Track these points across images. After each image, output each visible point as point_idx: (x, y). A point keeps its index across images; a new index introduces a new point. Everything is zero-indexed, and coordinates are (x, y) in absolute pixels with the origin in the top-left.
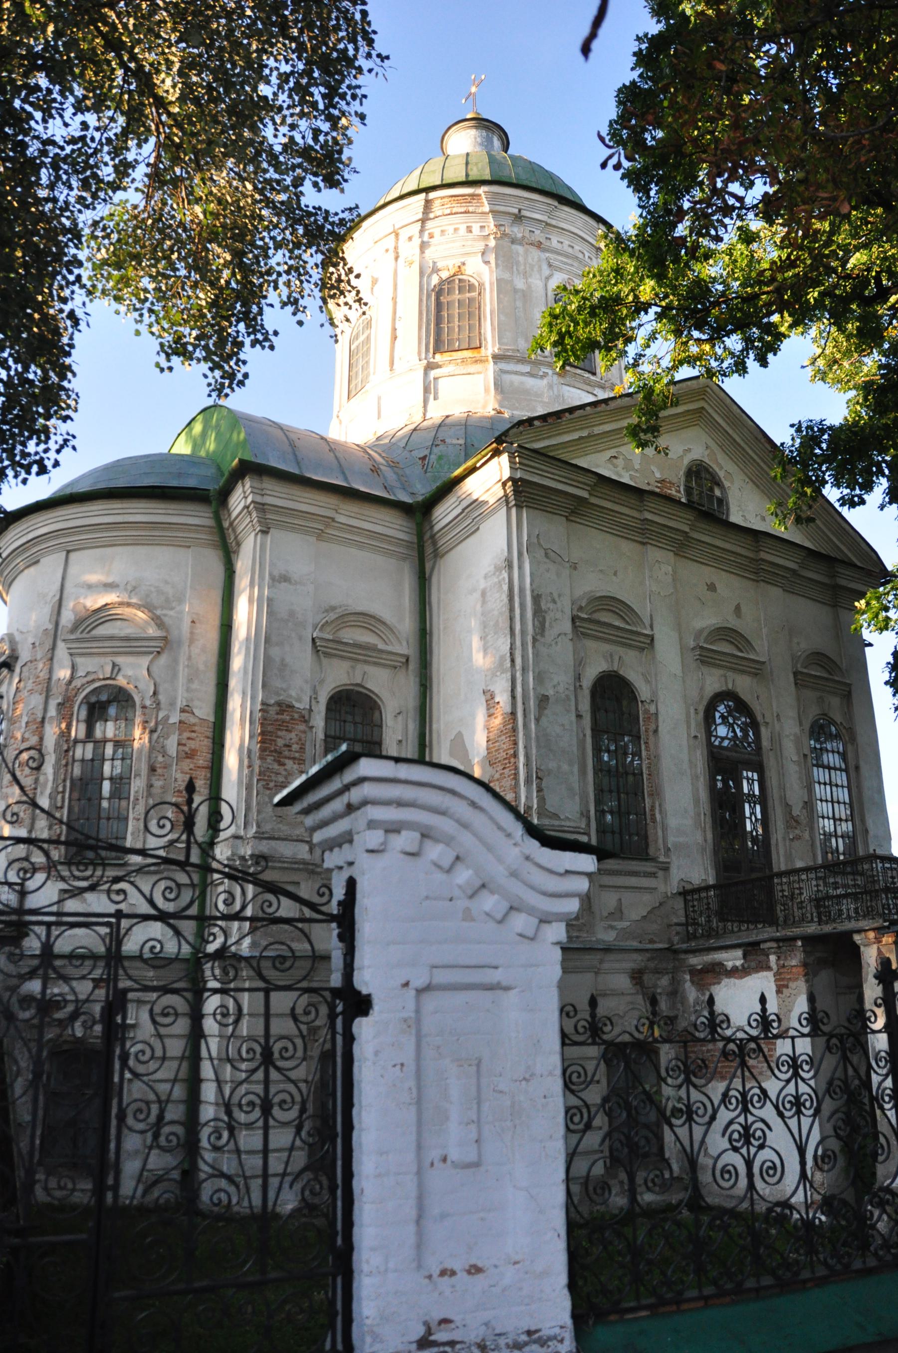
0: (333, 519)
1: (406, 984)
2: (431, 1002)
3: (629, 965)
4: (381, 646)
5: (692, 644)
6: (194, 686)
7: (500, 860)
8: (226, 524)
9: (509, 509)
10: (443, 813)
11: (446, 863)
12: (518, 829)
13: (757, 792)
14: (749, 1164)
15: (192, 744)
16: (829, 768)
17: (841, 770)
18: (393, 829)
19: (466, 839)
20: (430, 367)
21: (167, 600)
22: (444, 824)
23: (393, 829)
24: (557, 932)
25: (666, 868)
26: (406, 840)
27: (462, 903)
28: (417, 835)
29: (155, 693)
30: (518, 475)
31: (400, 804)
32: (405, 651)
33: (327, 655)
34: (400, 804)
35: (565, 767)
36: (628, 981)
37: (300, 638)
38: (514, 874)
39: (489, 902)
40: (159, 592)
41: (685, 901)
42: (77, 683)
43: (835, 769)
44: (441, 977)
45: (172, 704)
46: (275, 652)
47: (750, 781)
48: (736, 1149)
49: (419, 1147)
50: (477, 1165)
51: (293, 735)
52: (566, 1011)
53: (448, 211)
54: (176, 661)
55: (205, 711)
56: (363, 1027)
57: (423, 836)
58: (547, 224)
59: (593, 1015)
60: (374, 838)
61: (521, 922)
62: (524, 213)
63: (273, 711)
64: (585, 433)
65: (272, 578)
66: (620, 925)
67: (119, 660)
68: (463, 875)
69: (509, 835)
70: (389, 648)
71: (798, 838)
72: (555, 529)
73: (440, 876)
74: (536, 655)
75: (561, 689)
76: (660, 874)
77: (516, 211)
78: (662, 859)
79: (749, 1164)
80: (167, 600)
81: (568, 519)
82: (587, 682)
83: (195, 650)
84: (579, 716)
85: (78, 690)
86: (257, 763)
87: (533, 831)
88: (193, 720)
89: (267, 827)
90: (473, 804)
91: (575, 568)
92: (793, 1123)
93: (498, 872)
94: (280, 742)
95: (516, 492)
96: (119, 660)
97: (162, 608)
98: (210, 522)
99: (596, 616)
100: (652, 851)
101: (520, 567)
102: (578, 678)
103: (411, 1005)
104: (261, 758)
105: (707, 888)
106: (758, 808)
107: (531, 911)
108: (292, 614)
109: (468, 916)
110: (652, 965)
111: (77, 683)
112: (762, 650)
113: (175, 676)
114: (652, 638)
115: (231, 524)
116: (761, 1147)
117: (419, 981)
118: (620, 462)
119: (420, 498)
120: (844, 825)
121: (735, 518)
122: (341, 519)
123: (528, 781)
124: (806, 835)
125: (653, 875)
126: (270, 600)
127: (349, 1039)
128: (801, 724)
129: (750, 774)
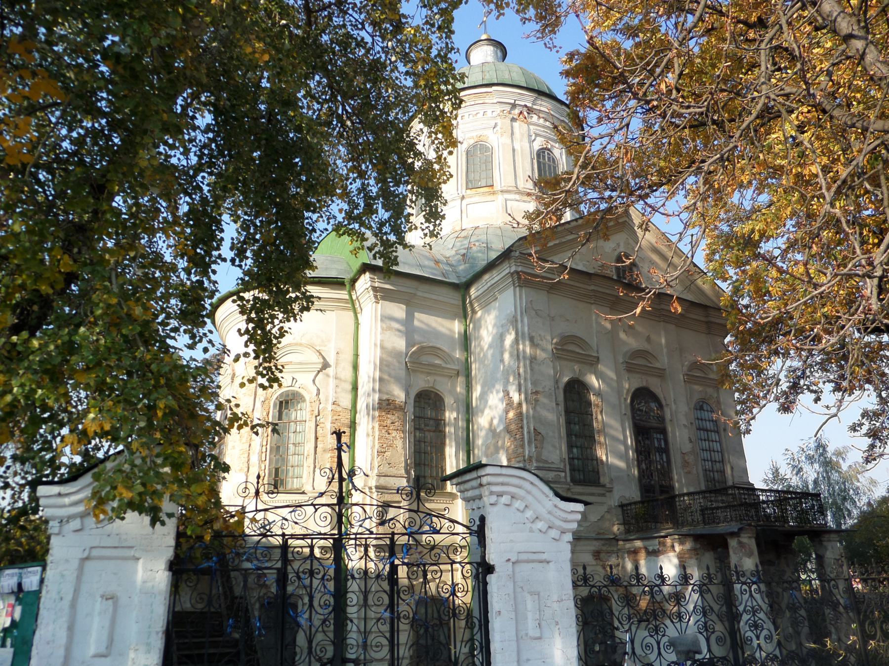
0: (415, 295)
1: (509, 560)
2: (518, 568)
3: (594, 548)
4: (444, 365)
5: (621, 360)
7: (544, 507)
8: (354, 297)
9: (515, 287)
10: (520, 487)
11: (522, 508)
12: (551, 494)
13: (663, 446)
14: (658, 643)
16: (707, 431)
17: (714, 431)
18: (500, 495)
19: (530, 498)
20: (463, 198)
22: (521, 492)
23: (500, 495)
24: (569, 537)
25: (610, 490)
26: (505, 499)
27: (529, 525)
28: (509, 497)
29: (318, 394)
30: (520, 269)
31: (502, 484)
32: (456, 368)
33: (413, 371)
34: (502, 484)
35: (551, 434)
36: (591, 557)
38: (550, 513)
39: (540, 525)
41: (623, 511)
43: (711, 431)
44: (523, 557)
45: (327, 400)
47: (659, 440)
48: (652, 636)
49: (517, 630)
50: (540, 638)
52: (574, 571)
53: (473, 103)
56: (491, 579)
57: (512, 497)
59: (585, 573)
60: (493, 499)
61: (554, 533)
62: (517, 102)
64: (557, 242)
66: (587, 524)
68: (529, 514)
69: (547, 496)
70: (448, 366)
71: (689, 473)
72: (541, 298)
73: (519, 514)
74: (532, 370)
75: (547, 389)
76: (607, 494)
77: (513, 101)
78: (608, 485)
79: (658, 643)
81: (548, 292)
82: (562, 385)
84: (557, 404)
87: (557, 494)
88: (339, 409)
90: (532, 483)
91: (553, 320)
92: (678, 625)
93: (543, 512)
97: (320, 346)
98: (347, 297)
99: (565, 347)
100: (602, 480)
101: (522, 321)
102: (557, 382)
103: (511, 569)
104: (380, 430)
105: (635, 503)
106: (664, 456)
107: (557, 528)
109: (531, 531)
110: (604, 548)
112: (663, 361)
114: (598, 358)
115: (357, 298)
116: (664, 635)
117: (513, 560)
118: (577, 257)
119: (464, 280)
120: (718, 464)
122: (420, 294)
123: (530, 442)
124: (694, 471)
125: (603, 495)
127: (485, 584)
128: (688, 404)
129: (658, 436)
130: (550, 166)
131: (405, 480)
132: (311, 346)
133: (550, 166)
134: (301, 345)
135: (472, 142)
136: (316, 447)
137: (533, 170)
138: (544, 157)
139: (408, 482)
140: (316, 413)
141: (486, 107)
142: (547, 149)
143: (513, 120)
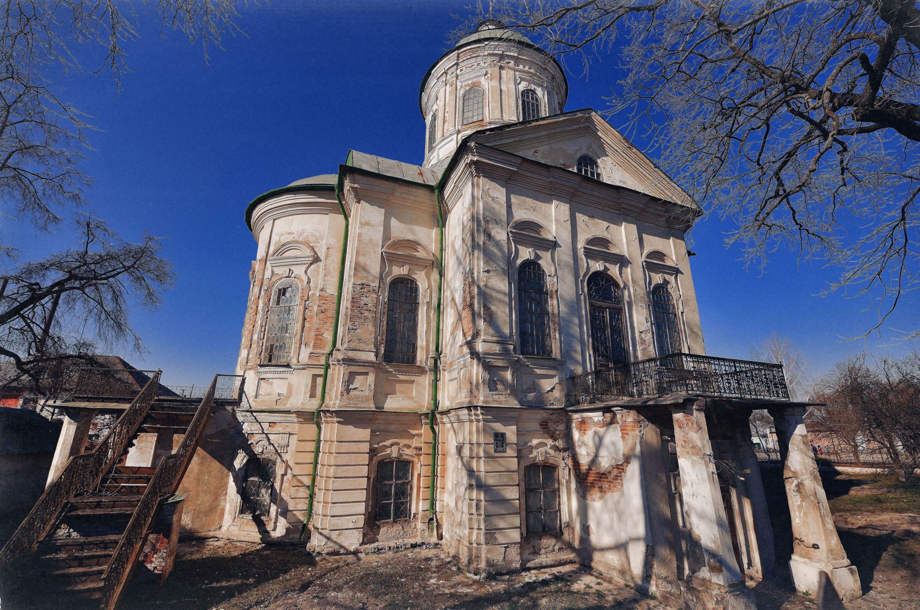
6: (327, 278)
15: (325, 306)
21: (317, 239)
29: (309, 282)
37: (375, 252)
40: (313, 235)
42: (274, 279)
45: (316, 287)
46: (362, 259)
51: (369, 299)
54: (318, 267)
55: (332, 290)
58: (517, 58)
63: (358, 287)
65: (361, 223)
67: (292, 268)
80: (317, 239)
83: (329, 262)
85: (276, 282)
86: (349, 312)
89: (353, 345)
94: (362, 303)
95: (476, 169)
96: (292, 268)
104: (352, 310)
108: (371, 240)
111: (274, 279)
113: (318, 274)
121: (606, 180)
126: (360, 235)
130: (533, 104)
131: (373, 354)
132: (307, 243)
133: (533, 104)
134: (297, 242)
135: (468, 88)
136: (303, 327)
137: (517, 106)
138: (528, 97)
139: (376, 356)
140: (306, 298)
141: (479, 59)
142: (531, 90)
143: (501, 68)
